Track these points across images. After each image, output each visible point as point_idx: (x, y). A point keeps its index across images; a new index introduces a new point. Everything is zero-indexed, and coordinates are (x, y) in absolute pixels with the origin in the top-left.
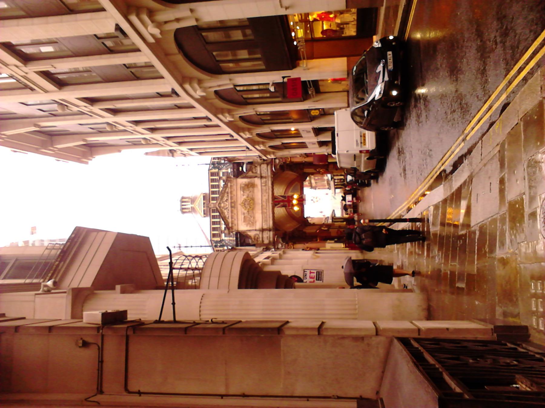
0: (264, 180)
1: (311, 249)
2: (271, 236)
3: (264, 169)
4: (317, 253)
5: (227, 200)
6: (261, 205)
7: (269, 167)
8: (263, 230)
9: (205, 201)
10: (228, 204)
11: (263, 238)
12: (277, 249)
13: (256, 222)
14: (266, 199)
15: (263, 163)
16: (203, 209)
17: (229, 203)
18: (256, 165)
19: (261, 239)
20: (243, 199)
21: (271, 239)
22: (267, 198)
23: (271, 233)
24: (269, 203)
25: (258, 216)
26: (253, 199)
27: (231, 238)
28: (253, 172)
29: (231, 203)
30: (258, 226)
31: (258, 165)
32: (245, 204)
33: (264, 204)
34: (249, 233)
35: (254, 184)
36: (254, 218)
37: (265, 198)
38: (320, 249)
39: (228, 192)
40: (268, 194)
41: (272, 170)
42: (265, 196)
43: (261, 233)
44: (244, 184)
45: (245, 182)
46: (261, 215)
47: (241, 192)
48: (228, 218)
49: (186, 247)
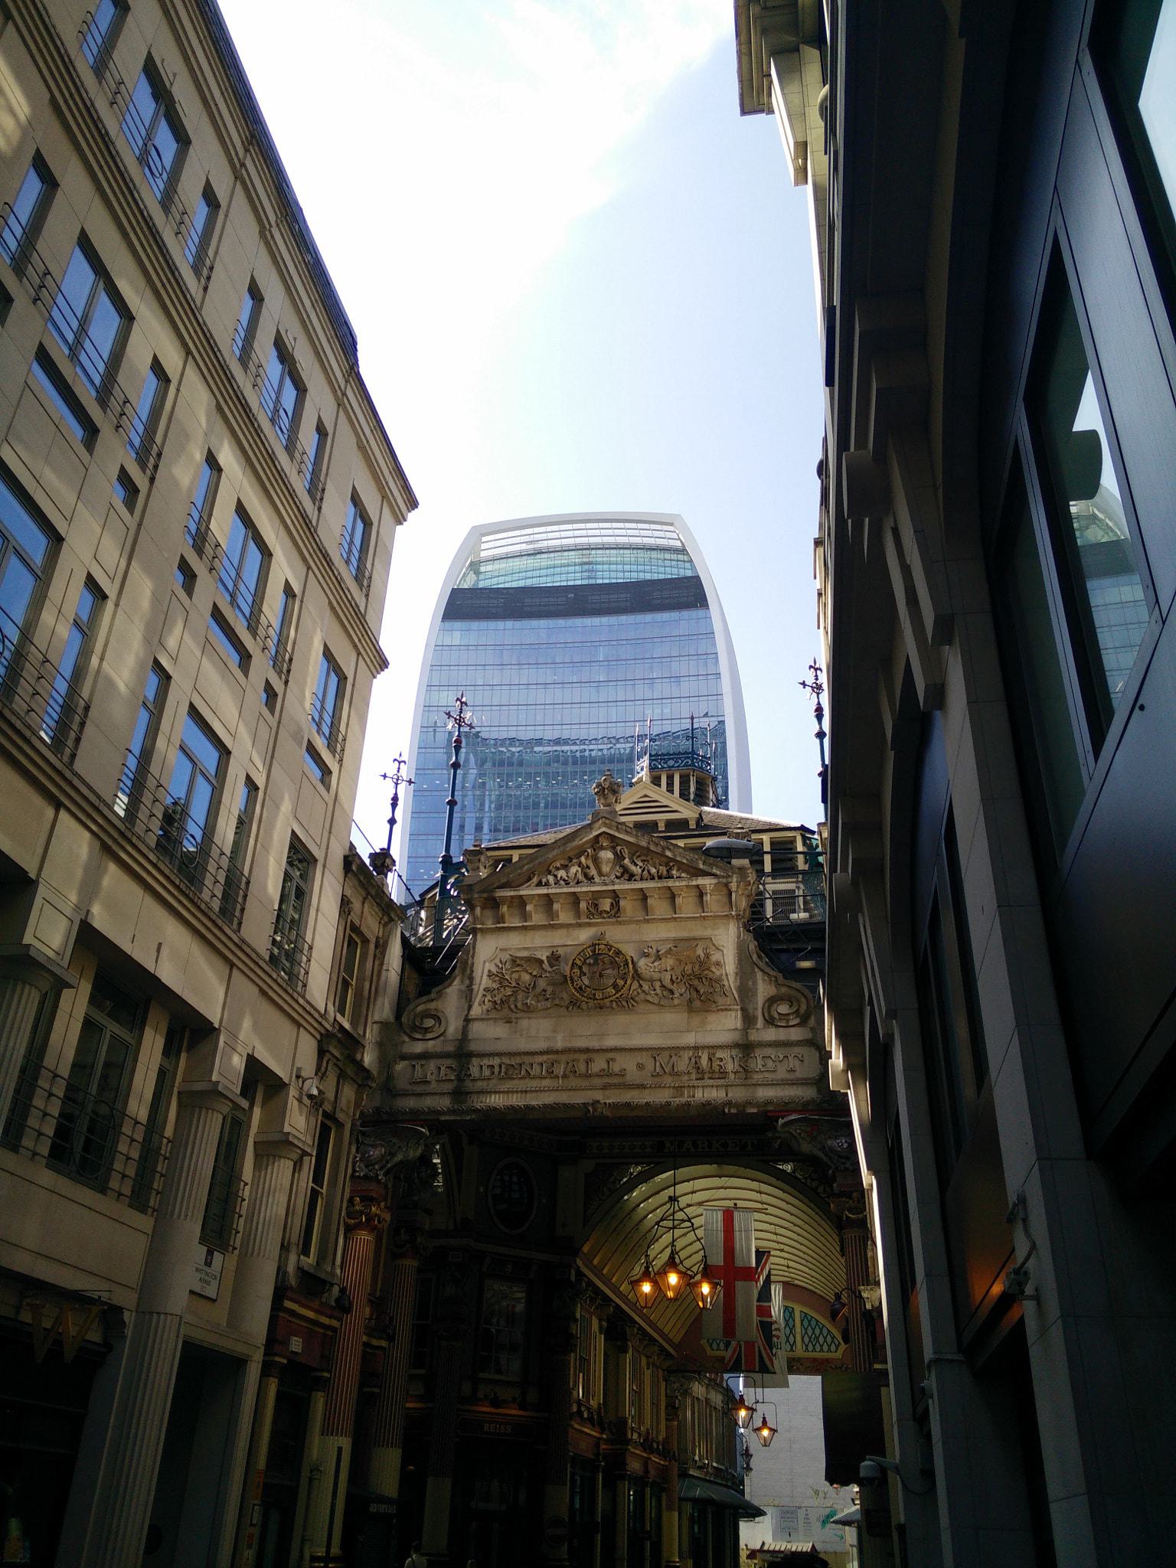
0: (730, 1063)
2: (428, 1102)
3: (793, 1063)
6: (594, 1044)
8: (462, 1054)
13: (509, 1022)
14: (622, 1073)
17: (613, 883)
20: (630, 951)
21: (410, 1103)
22: (628, 1078)
23: (445, 1103)
24: (605, 1087)
26: (626, 1003)
28: (771, 1001)
30: (489, 1033)
33: (599, 1064)
39: (670, 877)
40: (649, 1082)
41: (785, 1107)
42: (640, 1067)
43: (450, 1048)
44: (707, 956)
46: (542, 1045)
47: (666, 940)
48: (539, 884)
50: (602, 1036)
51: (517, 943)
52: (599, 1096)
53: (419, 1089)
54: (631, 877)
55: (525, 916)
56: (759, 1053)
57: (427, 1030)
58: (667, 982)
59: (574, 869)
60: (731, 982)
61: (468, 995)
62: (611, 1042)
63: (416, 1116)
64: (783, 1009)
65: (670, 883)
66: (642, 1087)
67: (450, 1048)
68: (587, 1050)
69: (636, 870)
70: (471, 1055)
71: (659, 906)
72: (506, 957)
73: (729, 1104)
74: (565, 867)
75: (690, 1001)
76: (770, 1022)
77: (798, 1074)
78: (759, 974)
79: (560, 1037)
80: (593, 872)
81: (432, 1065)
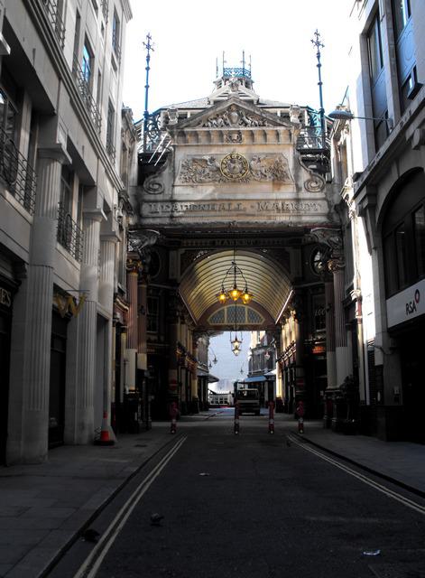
2: (158, 221)
6: (232, 197)
7: (323, 219)
11: (156, 201)
13: (192, 186)
14: (245, 210)
15: (330, 206)
18: (325, 191)
19: (152, 197)
21: (150, 221)
22: (248, 212)
23: (167, 221)
24: (237, 215)
25: (206, 192)
26: (246, 180)
28: (309, 181)
31: (326, 194)
35: (280, 185)
41: (313, 225)
42: (252, 207)
45: (285, 165)
47: (263, 154)
48: (204, 126)
51: (193, 152)
52: (235, 219)
53: (155, 215)
54: (246, 125)
55: (198, 140)
56: (302, 202)
57: (155, 190)
58: (263, 172)
59: (220, 120)
60: (291, 173)
62: (240, 196)
63: (153, 226)
64: (313, 185)
65: (264, 128)
66: (253, 215)
67: (168, 198)
68: (229, 200)
69: (249, 122)
70: (175, 201)
71: (259, 138)
72: (190, 158)
73: (291, 223)
74: (215, 119)
75: (273, 180)
76: (308, 190)
77: (319, 211)
78: (303, 170)
79: (216, 194)
80: (228, 121)
81: (159, 205)
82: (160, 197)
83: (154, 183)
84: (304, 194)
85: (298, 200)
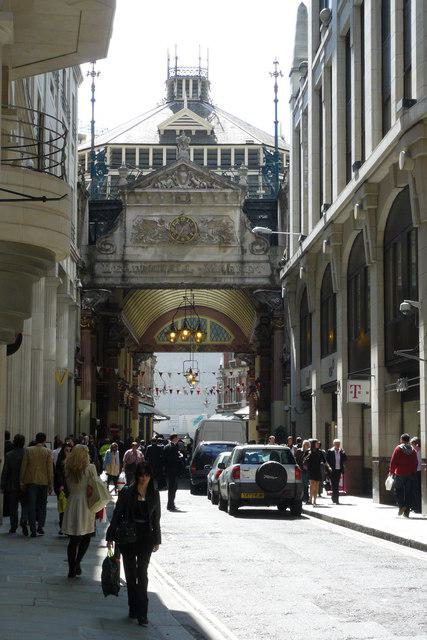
0: (236, 268)
1: (79, 366)
2: (110, 281)
4: (70, 379)
5: (195, 186)
7: (266, 281)
8: (124, 262)
9: (194, 133)
10: (183, 188)
11: (108, 261)
12: (82, 292)
15: (272, 269)
16: (178, 128)
19: (104, 257)
20: (194, 220)
21: (101, 281)
27: (108, 191)
29: (189, 194)
32: (182, 224)
34: (118, 232)
36: (152, 243)
37: (192, 267)
38: (79, 388)
48: (154, 187)
49: (93, 86)
50: (184, 256)
51: (143, 212)
54: (195, 186)
55: (149, 201)
60: (237, 235)
61: (125, 236)
62: (187, 258)
64: (258, 247)
65: (212, 190)
67: (118, 258)
68: (177, 261)
76: (252, 252)
79: (166, 255)
80: (177, 182)
82: (111, 257)
83: (106, 243)
84: (249, 257)
85: (242, 262)
